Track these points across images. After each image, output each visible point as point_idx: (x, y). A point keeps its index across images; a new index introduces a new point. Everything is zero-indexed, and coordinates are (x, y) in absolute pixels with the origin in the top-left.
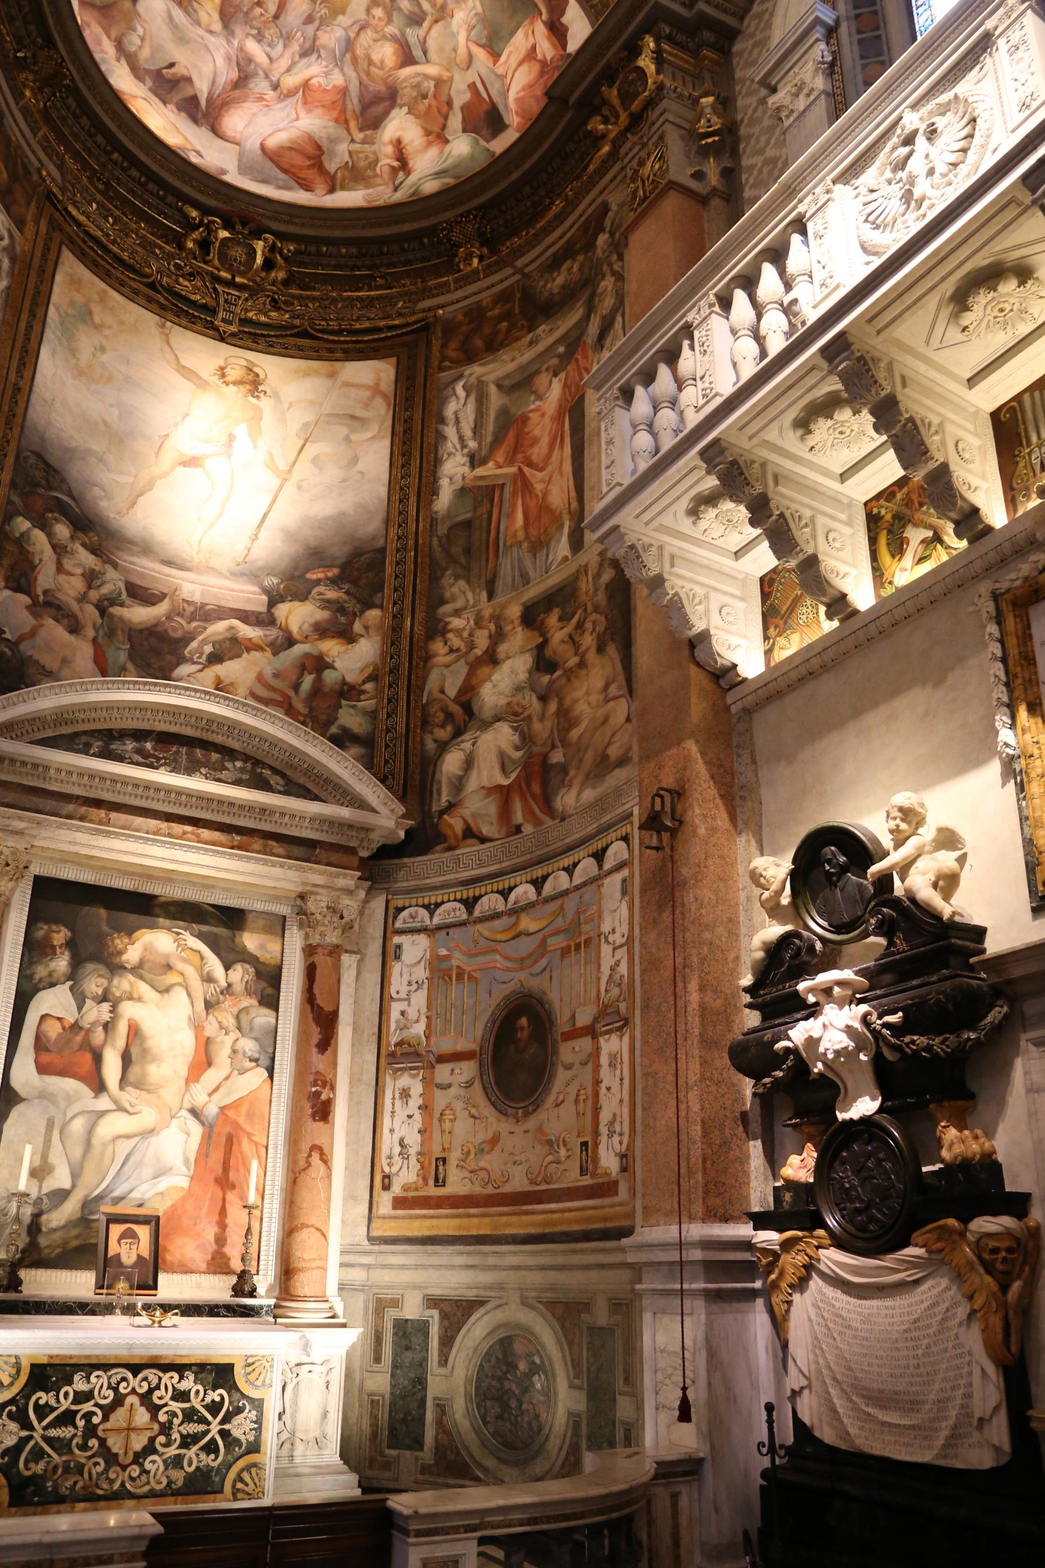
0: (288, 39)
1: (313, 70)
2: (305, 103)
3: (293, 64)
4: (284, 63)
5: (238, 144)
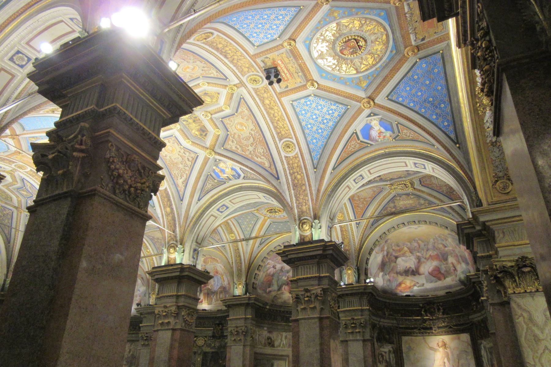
0: (423, 250)
1: (430, 253)
2: (432, 259)
3: (426, 253)
4: (425, 254)
5: (424, 274)
